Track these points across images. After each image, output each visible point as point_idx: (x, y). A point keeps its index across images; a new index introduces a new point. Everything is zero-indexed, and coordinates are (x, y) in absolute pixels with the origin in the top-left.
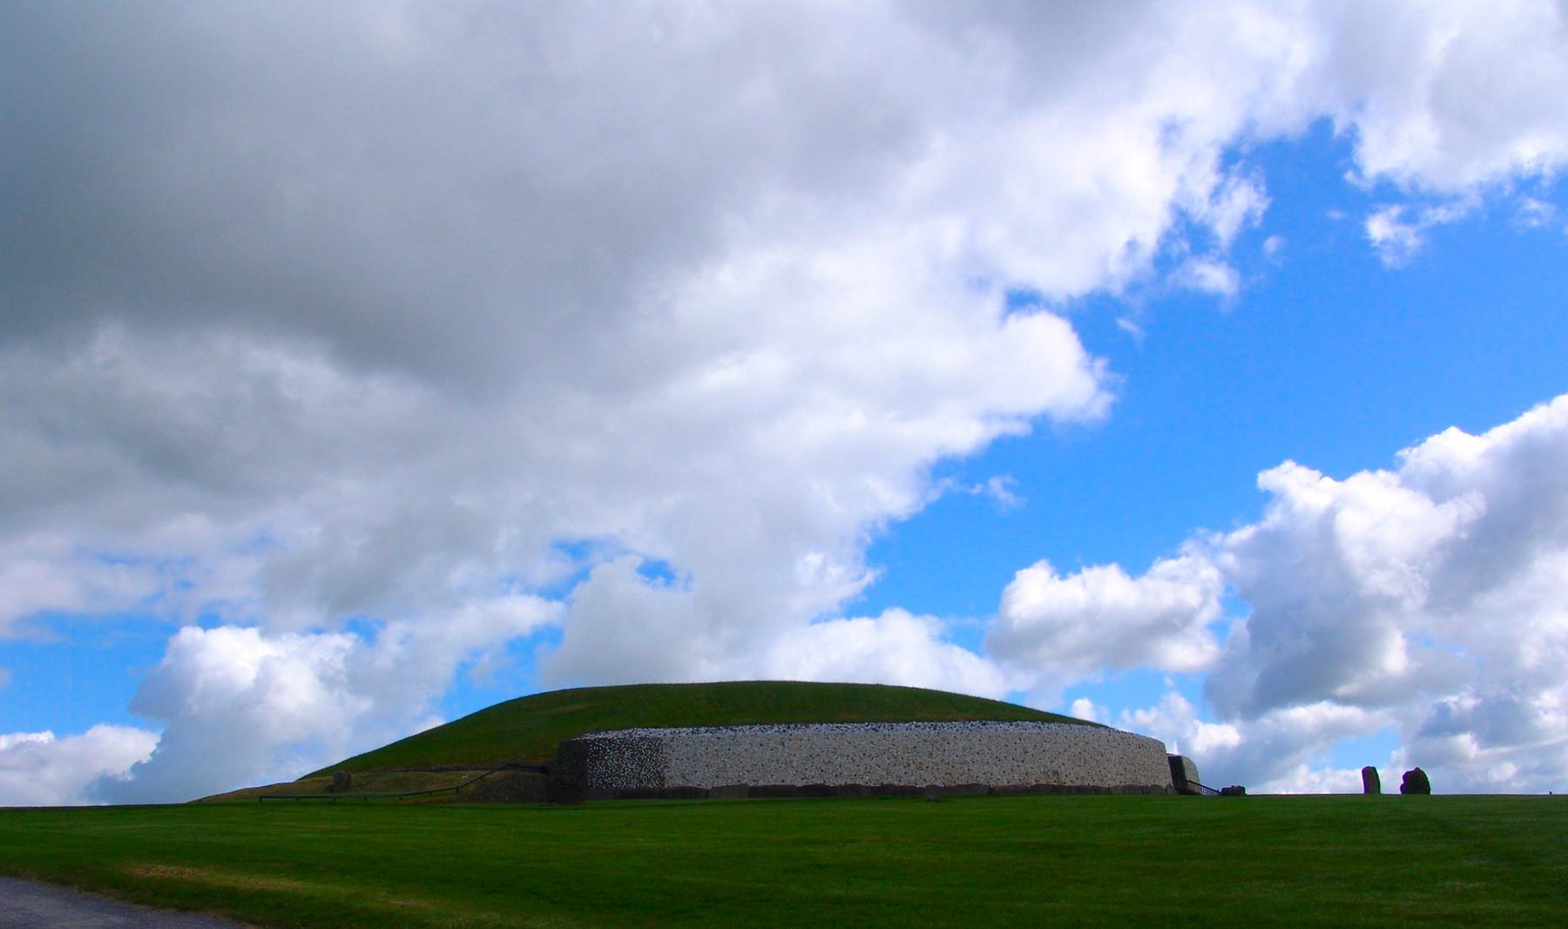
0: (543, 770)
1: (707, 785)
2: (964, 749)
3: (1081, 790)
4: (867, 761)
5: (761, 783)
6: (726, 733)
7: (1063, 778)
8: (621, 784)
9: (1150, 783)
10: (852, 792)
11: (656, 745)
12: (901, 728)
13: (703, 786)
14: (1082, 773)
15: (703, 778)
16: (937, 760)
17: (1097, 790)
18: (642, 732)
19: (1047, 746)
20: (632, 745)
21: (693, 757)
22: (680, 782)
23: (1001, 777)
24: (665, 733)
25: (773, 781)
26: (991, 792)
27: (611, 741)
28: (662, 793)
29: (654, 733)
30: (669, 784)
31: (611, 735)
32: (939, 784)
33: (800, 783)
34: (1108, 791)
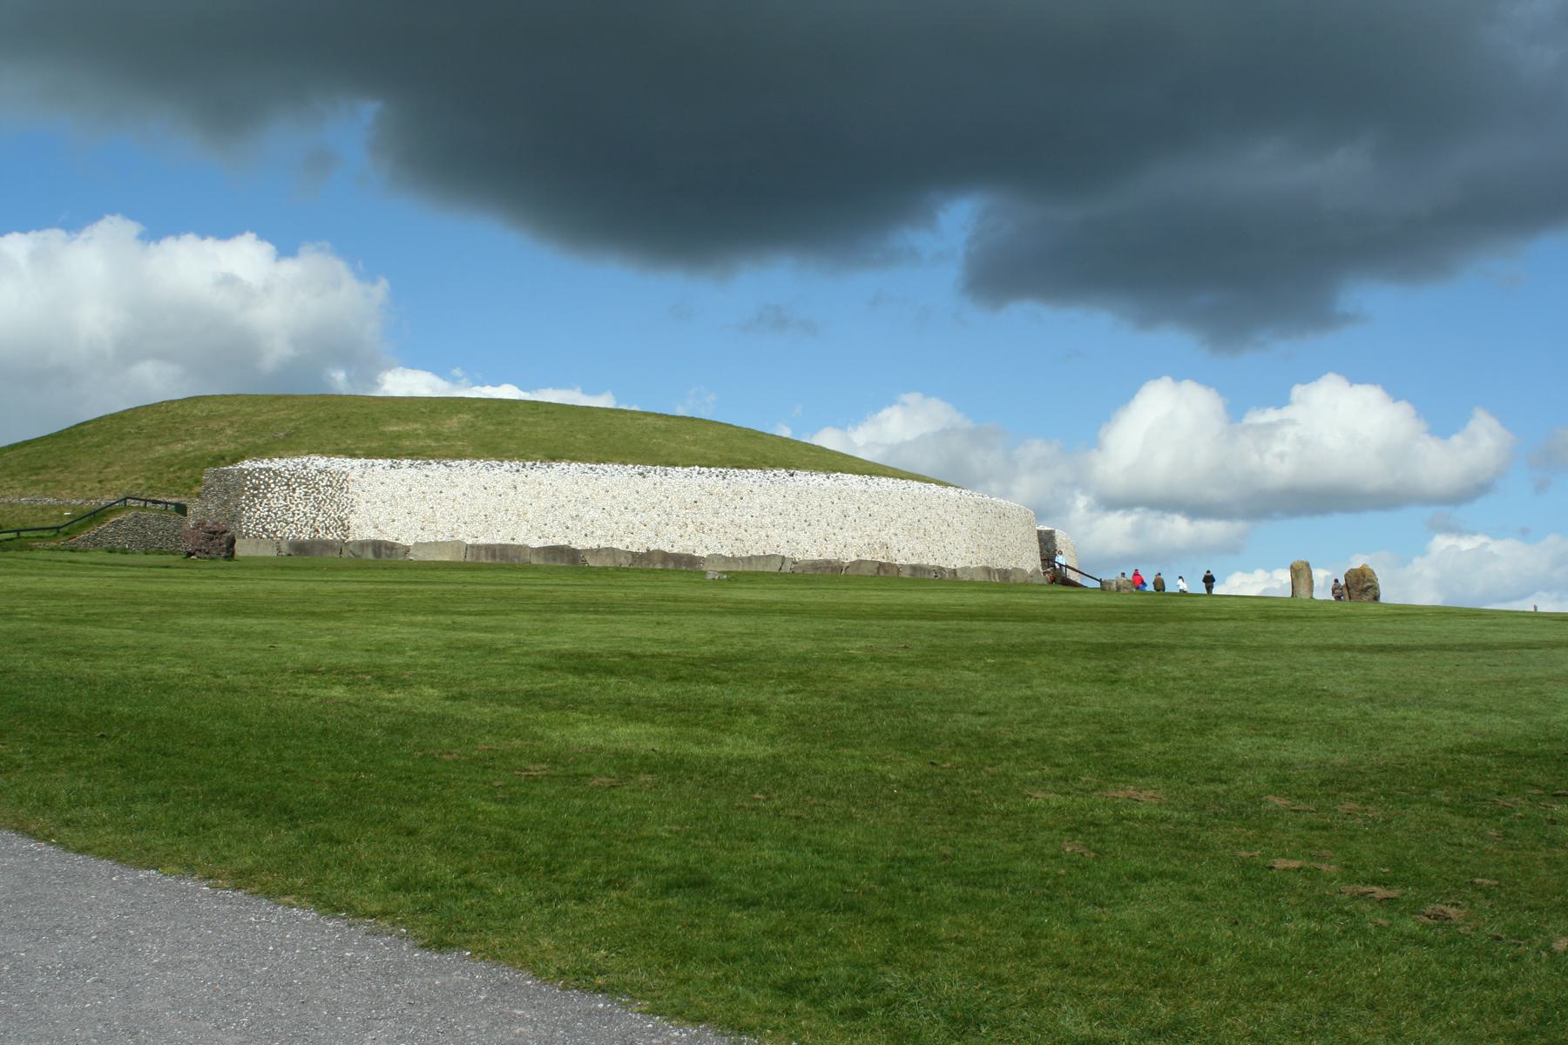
2: (762, 508)
4: (629, 516)
5: (482, 541)
6: (437, 471)
7: (893, 554)
8: (289, 533)
9: (1010, 565)
11: (340, 483)
12: (678, 473)
13: (403, 541)
14: (919, 548)
16: (726, 521)
18: (321, 462)
20: (305, 481)
22: (370, 534)
23: (808, 547)
24: (352, 467)
30: (357, 535)
32: (726, 552)
33: (536, 543)
34: (954, 571)
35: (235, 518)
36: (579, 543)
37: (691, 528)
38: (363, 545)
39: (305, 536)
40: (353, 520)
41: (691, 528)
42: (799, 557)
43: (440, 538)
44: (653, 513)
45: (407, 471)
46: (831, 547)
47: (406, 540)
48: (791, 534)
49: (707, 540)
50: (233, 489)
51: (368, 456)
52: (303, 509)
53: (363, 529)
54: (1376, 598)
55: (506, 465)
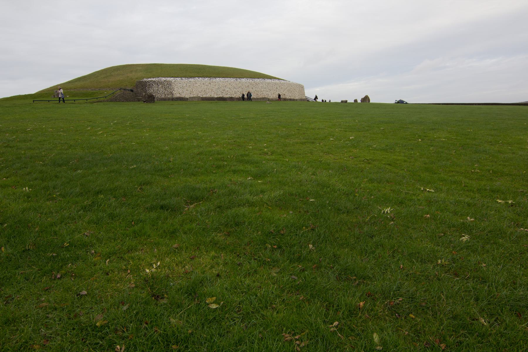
0: (132, 91)
1: (187, 96)
3: (290, 100)
4: (235, 90)
5: (204, 96)
6: (192, 80)
10: (231, 99)
11: (170, 83)
12: (243, 80)
13: (186, 97)
17: (294, 100)
18: (164, 79)
20: (161, 83)
21: (182, 87)
22: (178, 95)
25: (208, 96)
26: (269, 100)
27: (154, 82)
28: (173, 99)
31: (154, 79)
33: (216, 96)
36: (225, 96)
39: (163, 96)
54: (369, 101)
55: (207, 79)
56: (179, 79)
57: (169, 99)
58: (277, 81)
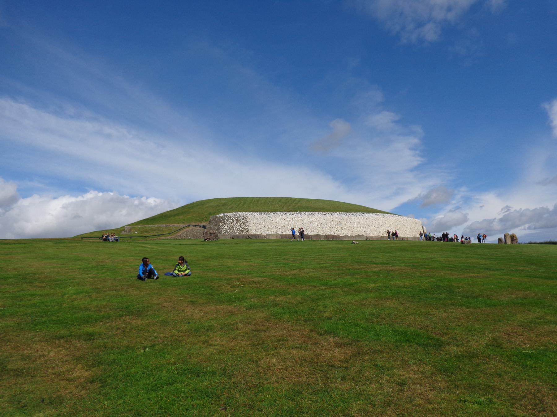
0: (204, 227)
4: (323, 226)
5: (284, 233)
6: (272, 215)
8: (232, 232)
11: (246, 219)
13: (263, 234)
15: (263, 231)
18: (241, 213)
19: (386, 222)
20: (237, 218)
22: (254, 232)
29: (245, 214)
32: (348, 235)
35: (219, 229)
37: (339, 229)
38: (252, 235)
40: (250, 229)
41: (339, 229)
42: (367, 235)
43: (273, 233)
44: (329, 225)
45: (264, 215)
46: (376, 233)
47: (264, 234)
48: (365, 229)
49: (343, 232)
50: (218, 222)
51: (253, 212)
52: (236, 226)
53: (252, 232)
55: (289, 213)
56: (256, 214)
57: (243, 236)
58: (379, 216)
